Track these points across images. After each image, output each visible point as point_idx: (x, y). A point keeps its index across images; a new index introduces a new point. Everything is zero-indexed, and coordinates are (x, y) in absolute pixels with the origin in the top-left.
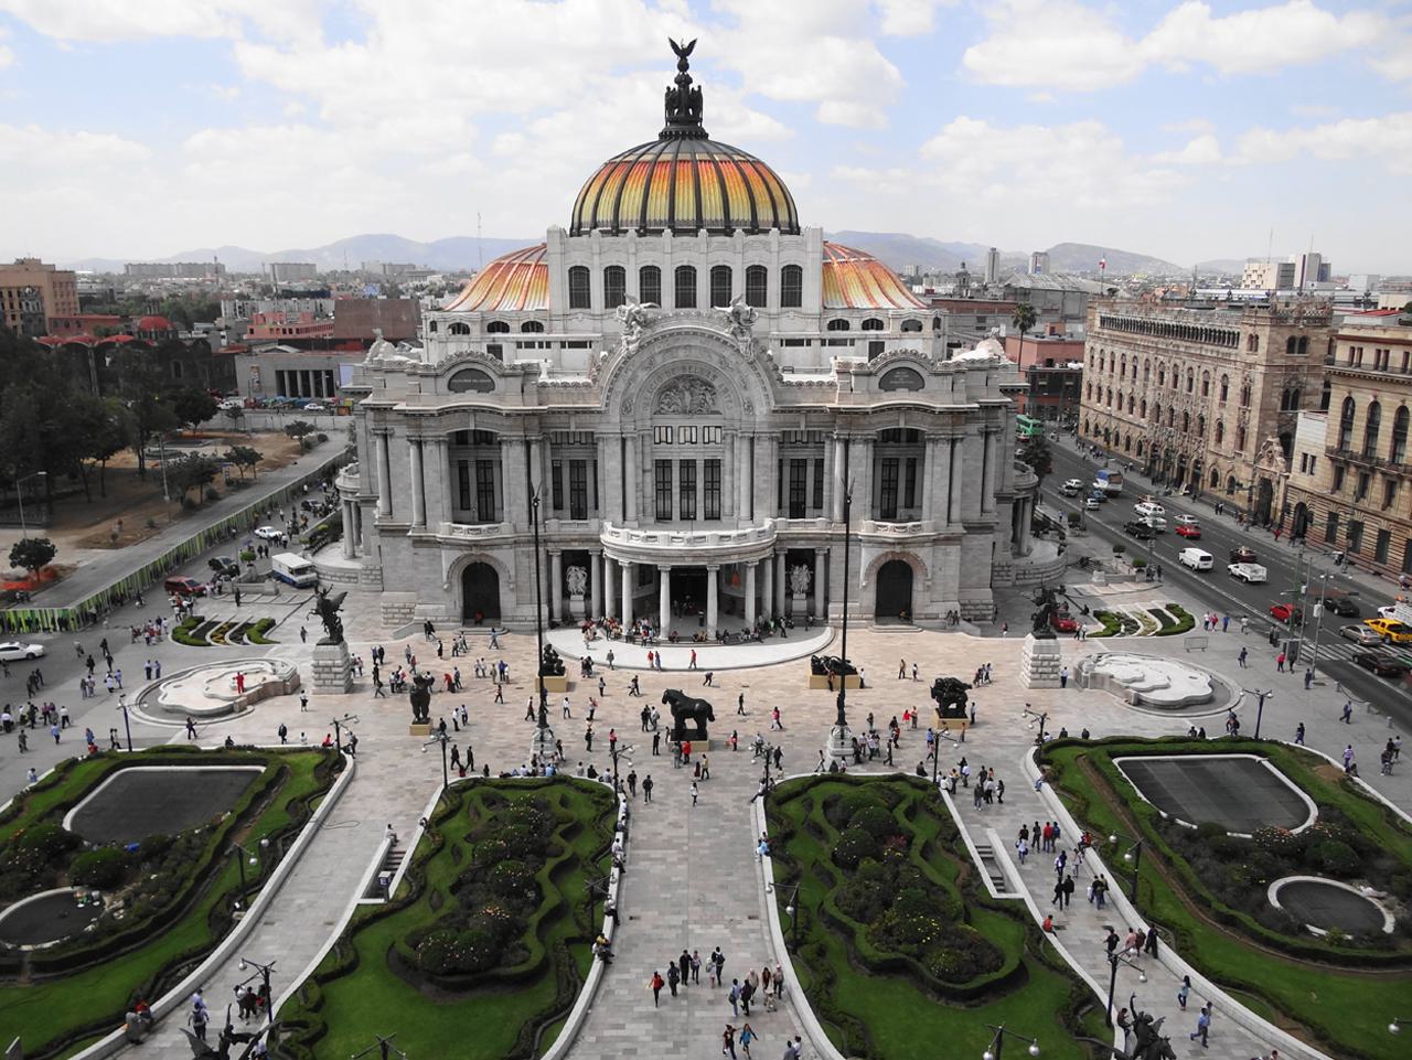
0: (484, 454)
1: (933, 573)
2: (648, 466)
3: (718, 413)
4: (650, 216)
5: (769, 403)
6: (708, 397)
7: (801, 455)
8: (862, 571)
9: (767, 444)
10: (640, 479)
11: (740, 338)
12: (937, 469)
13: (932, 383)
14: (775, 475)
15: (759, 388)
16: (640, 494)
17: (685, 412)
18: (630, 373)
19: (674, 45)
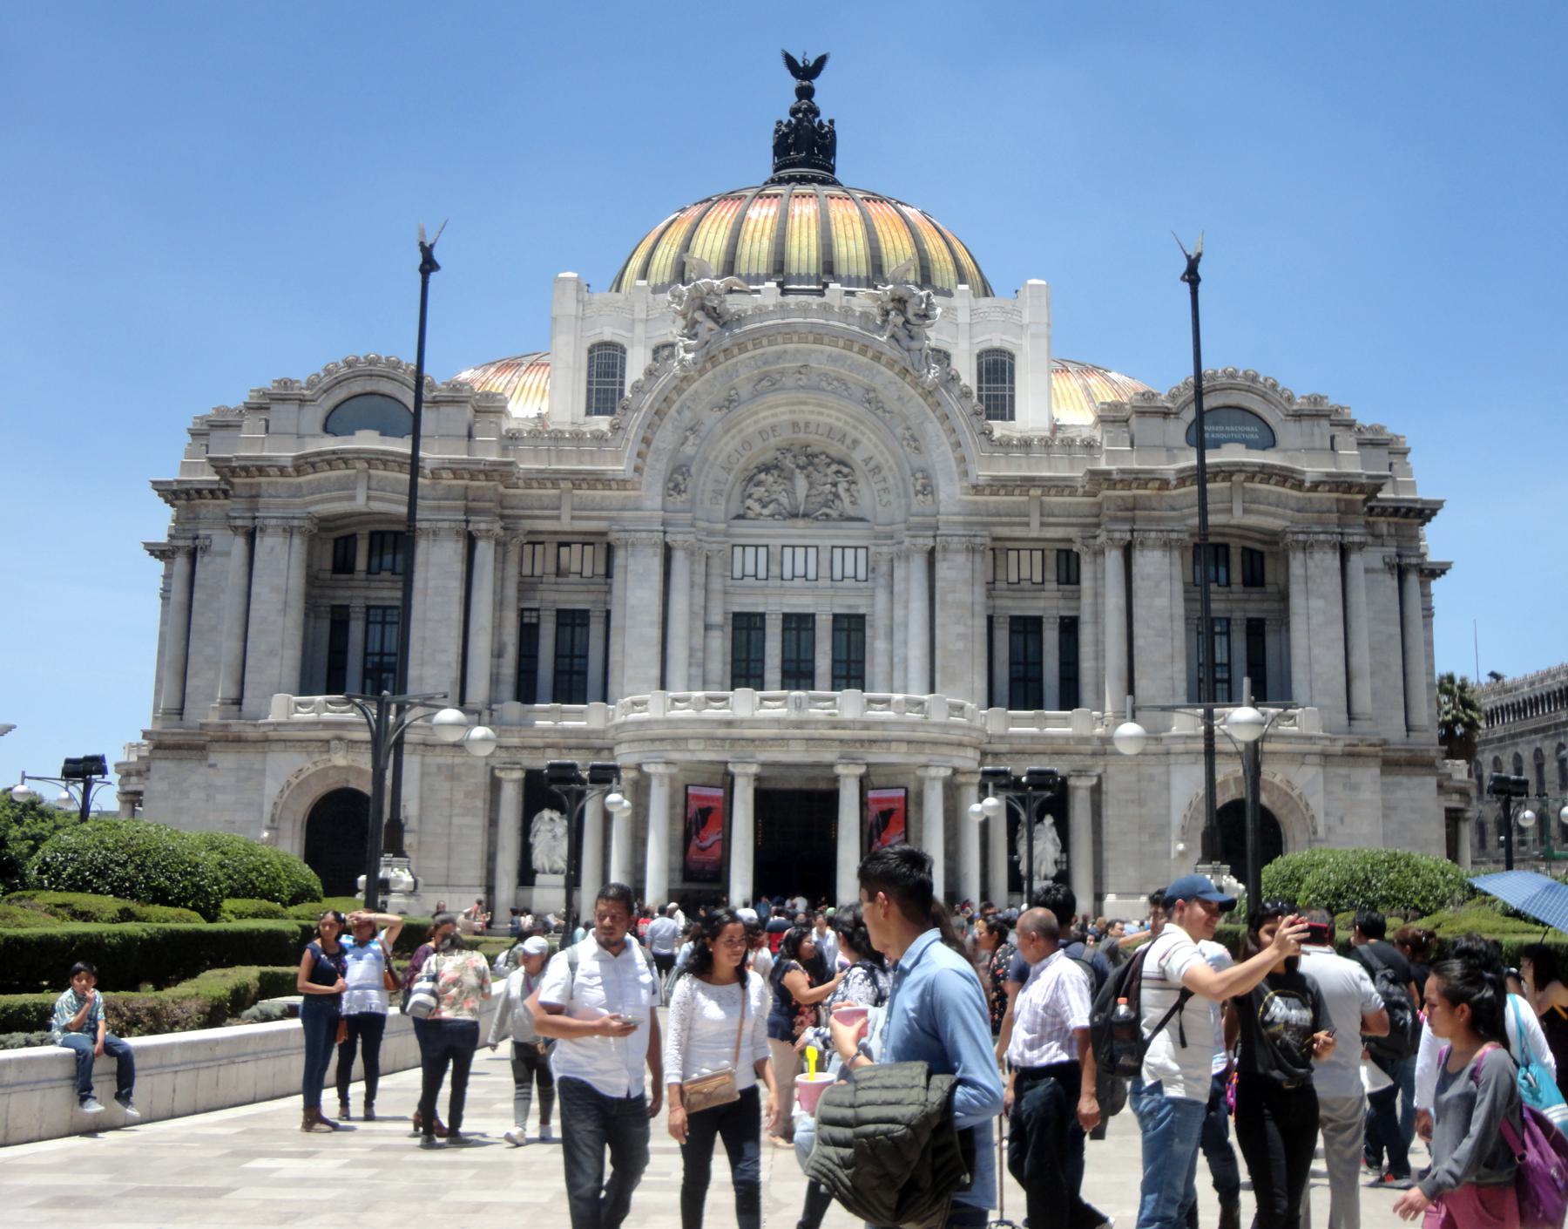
0: (388, 594)
1: (1329, 829)
2: (717, 617)
3: (862, 520)
4: (742, 267)
5: (965, 474)
6: (841, 489)
7: (1029, 608)
8: (1177, 819)
9: (961, 559)
10: (698, 641)
11: (906, 342)
12: (1316, 604)
13: (1288, 433)
14: (981, 624)
15: (947, 448)
16: (697, 671)
17: (795, 516)
18: (687, 414)
19: (790, 62)
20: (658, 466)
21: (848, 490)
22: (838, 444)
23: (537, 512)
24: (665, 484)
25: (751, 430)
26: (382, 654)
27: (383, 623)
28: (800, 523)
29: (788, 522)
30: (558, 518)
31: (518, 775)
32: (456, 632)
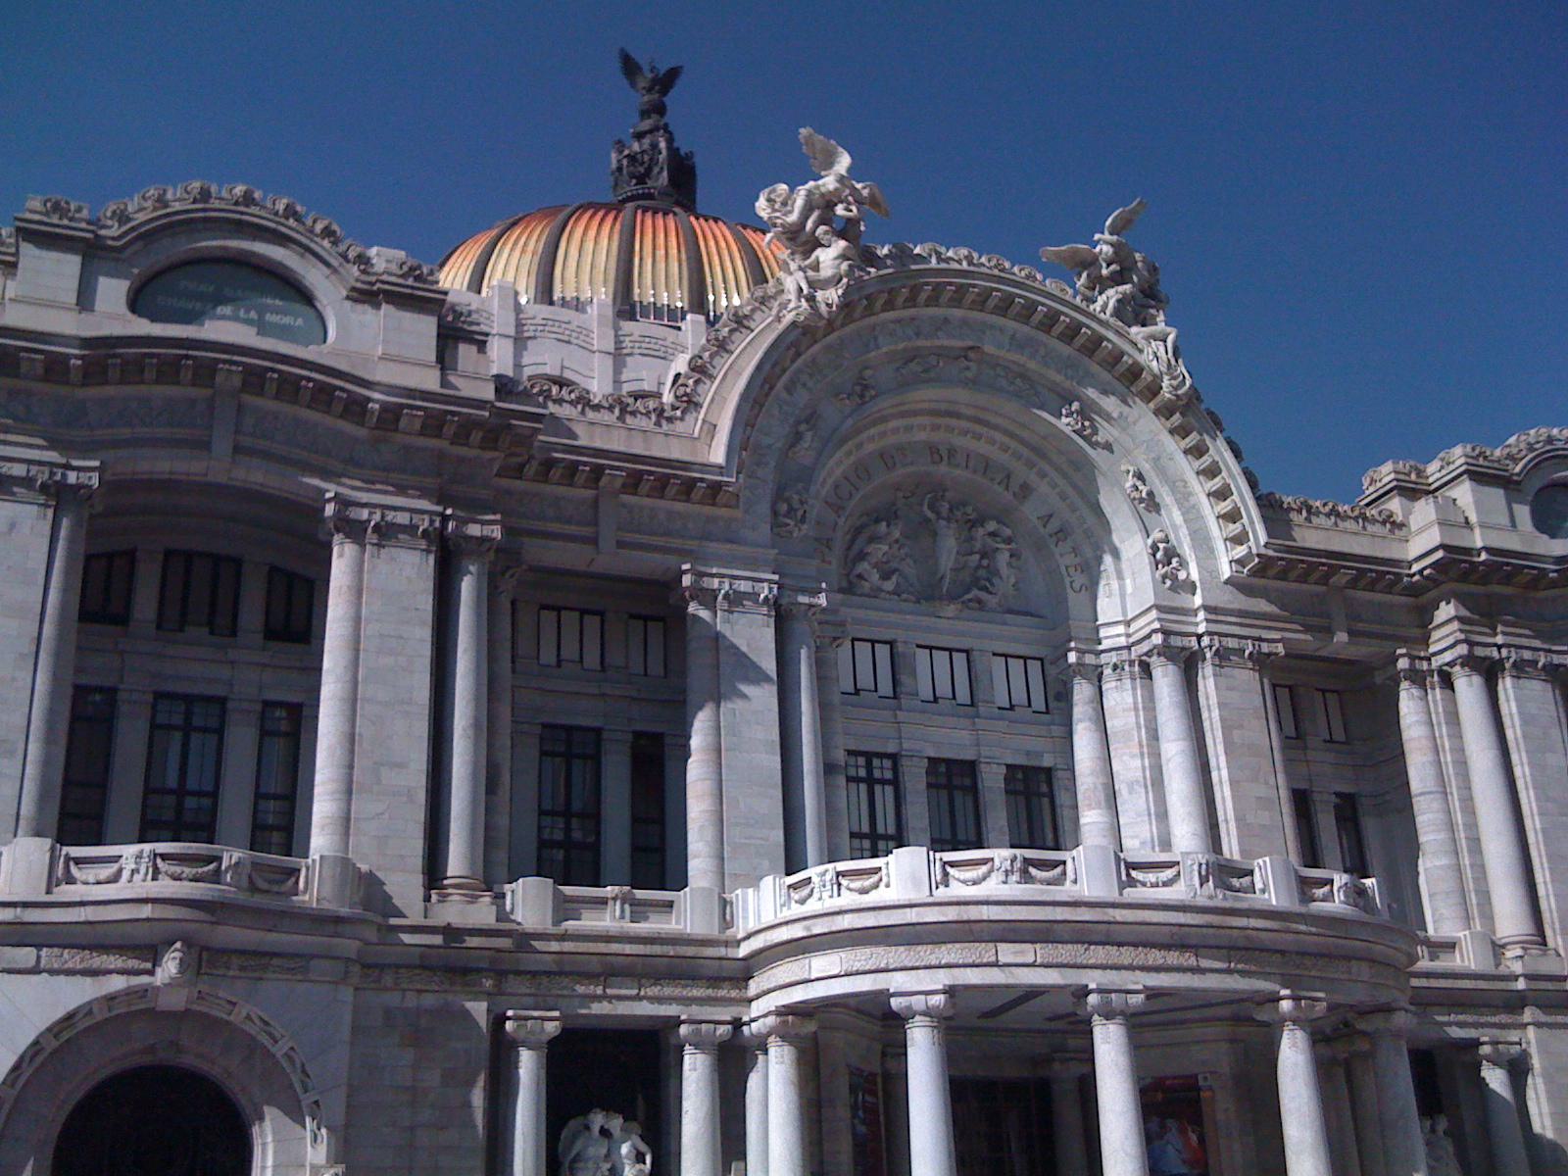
2: (840, 756)
4: (644, 292)
6: (1003, 559)
11: (1134, 330)
18: (802, 397)
20: (760, 473)
21: (1009, 565)
22: (1000, 489)
23: (555, 527)
24: (774, 505)
25: (870, 447)
26: (181, 792)
27: (187, 729)
28: (951, 609)
29: (924, 606)
30: (594, 541)
31: (552, 1028)
32: (422, 728)
